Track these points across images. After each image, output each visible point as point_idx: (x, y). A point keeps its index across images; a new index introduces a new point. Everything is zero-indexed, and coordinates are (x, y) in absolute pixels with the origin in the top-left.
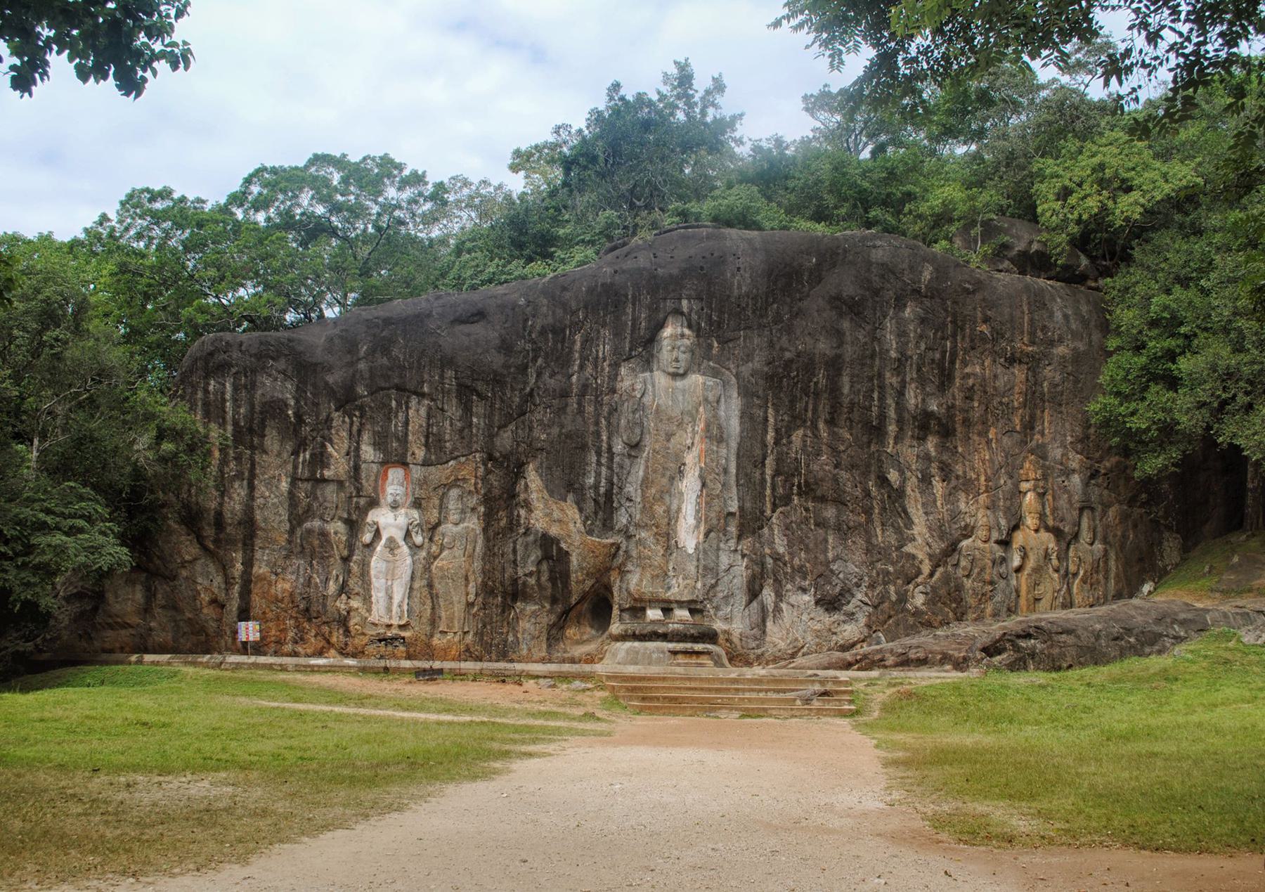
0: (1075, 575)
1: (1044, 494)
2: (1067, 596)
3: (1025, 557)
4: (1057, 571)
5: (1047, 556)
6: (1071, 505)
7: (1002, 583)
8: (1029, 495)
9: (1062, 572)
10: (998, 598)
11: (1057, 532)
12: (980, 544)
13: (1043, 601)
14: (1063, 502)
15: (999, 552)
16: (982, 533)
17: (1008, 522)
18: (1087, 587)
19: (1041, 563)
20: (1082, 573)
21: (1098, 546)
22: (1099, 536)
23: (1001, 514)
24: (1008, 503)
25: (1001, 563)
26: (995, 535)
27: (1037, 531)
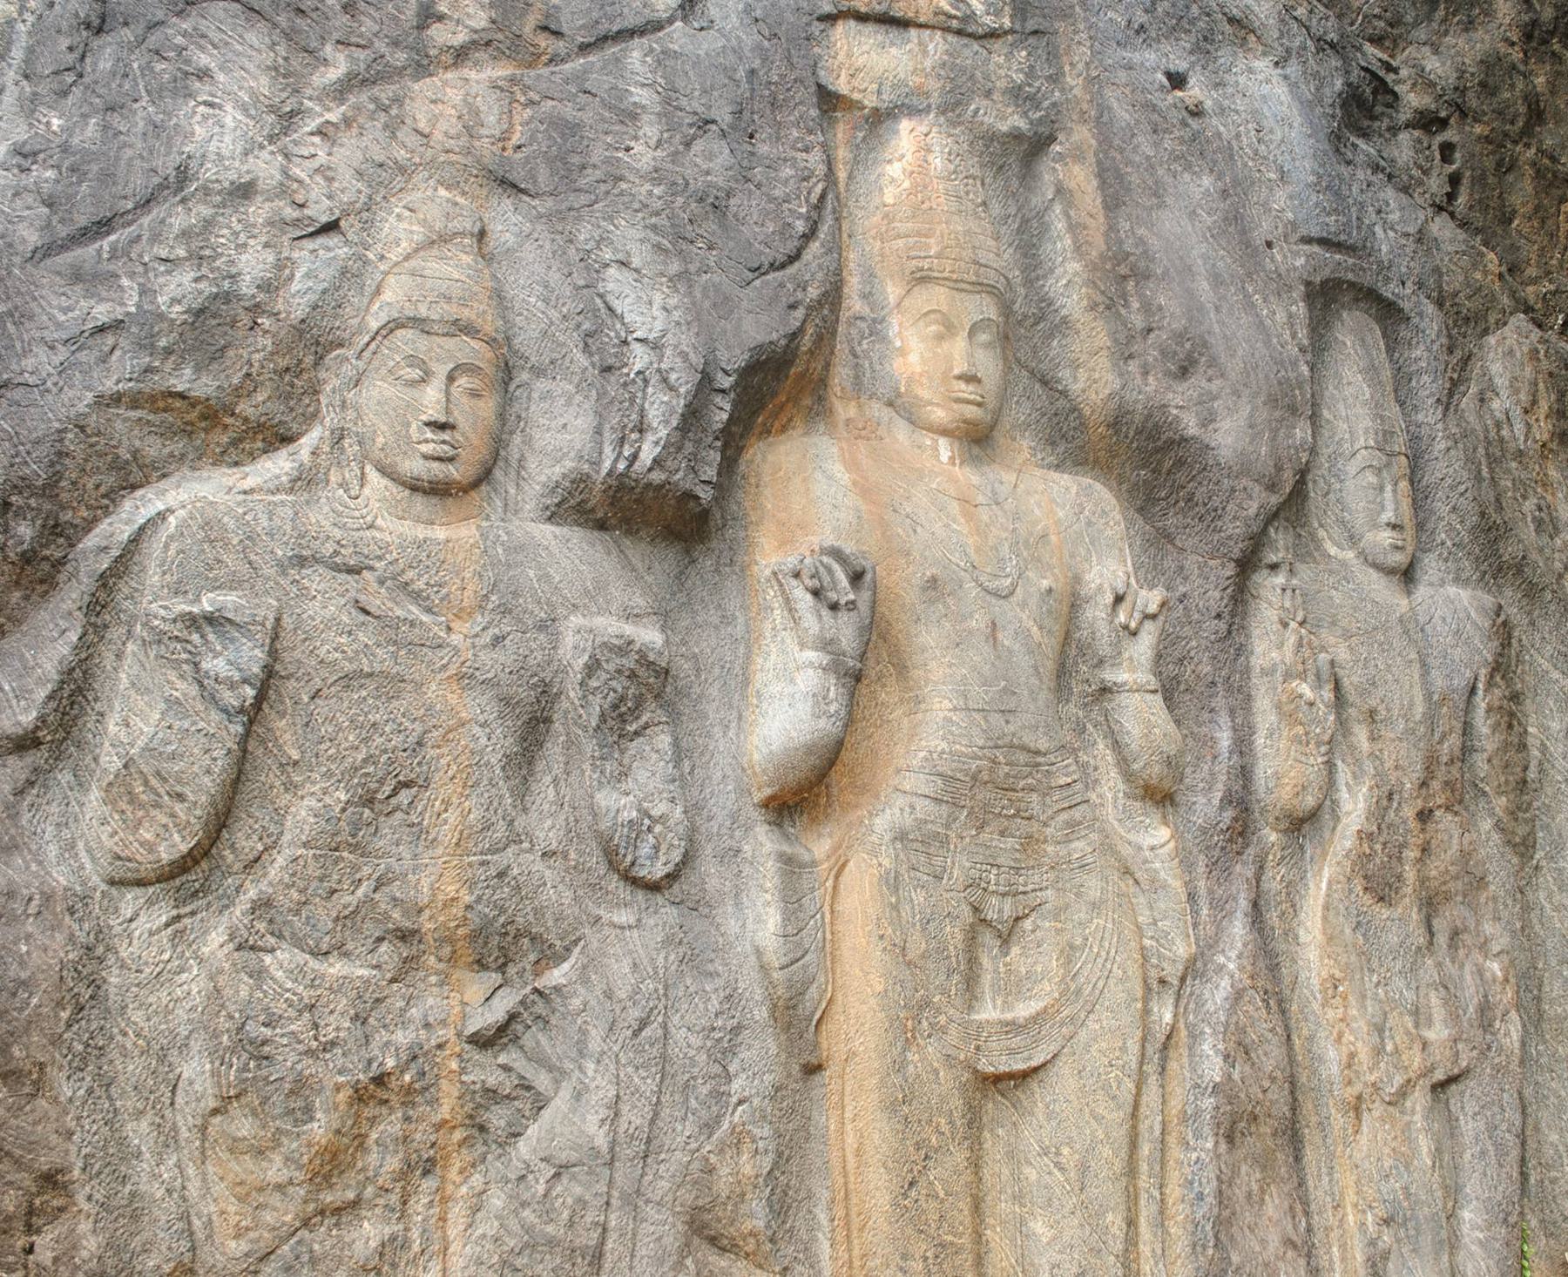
0: (1303, 824)
1: (1032, 147)
2: (1262, 1024)
3: (866, 668)
4: (1160, 796)
5: (1072, 666)
6: (1250, 251)
7: (626, 946)
8: (907, 136)
9: (1206, 805)
10: (571, 1120)
11: (1150, 465)
12: (378, 514)
13: (1063, 1085)
14: (1182, 223)
15: (598, 602)
16: (393, 401)
17: (707, 314)
18: (1400, 922)
19: (1032, 723)
20: (1354, 806)
21: (1452, 603)
22: (1451, 517)
23: (631, 237)
24: (712, 161)
25: (620, 723)
26: (562, 435)
27: (977, 439)
